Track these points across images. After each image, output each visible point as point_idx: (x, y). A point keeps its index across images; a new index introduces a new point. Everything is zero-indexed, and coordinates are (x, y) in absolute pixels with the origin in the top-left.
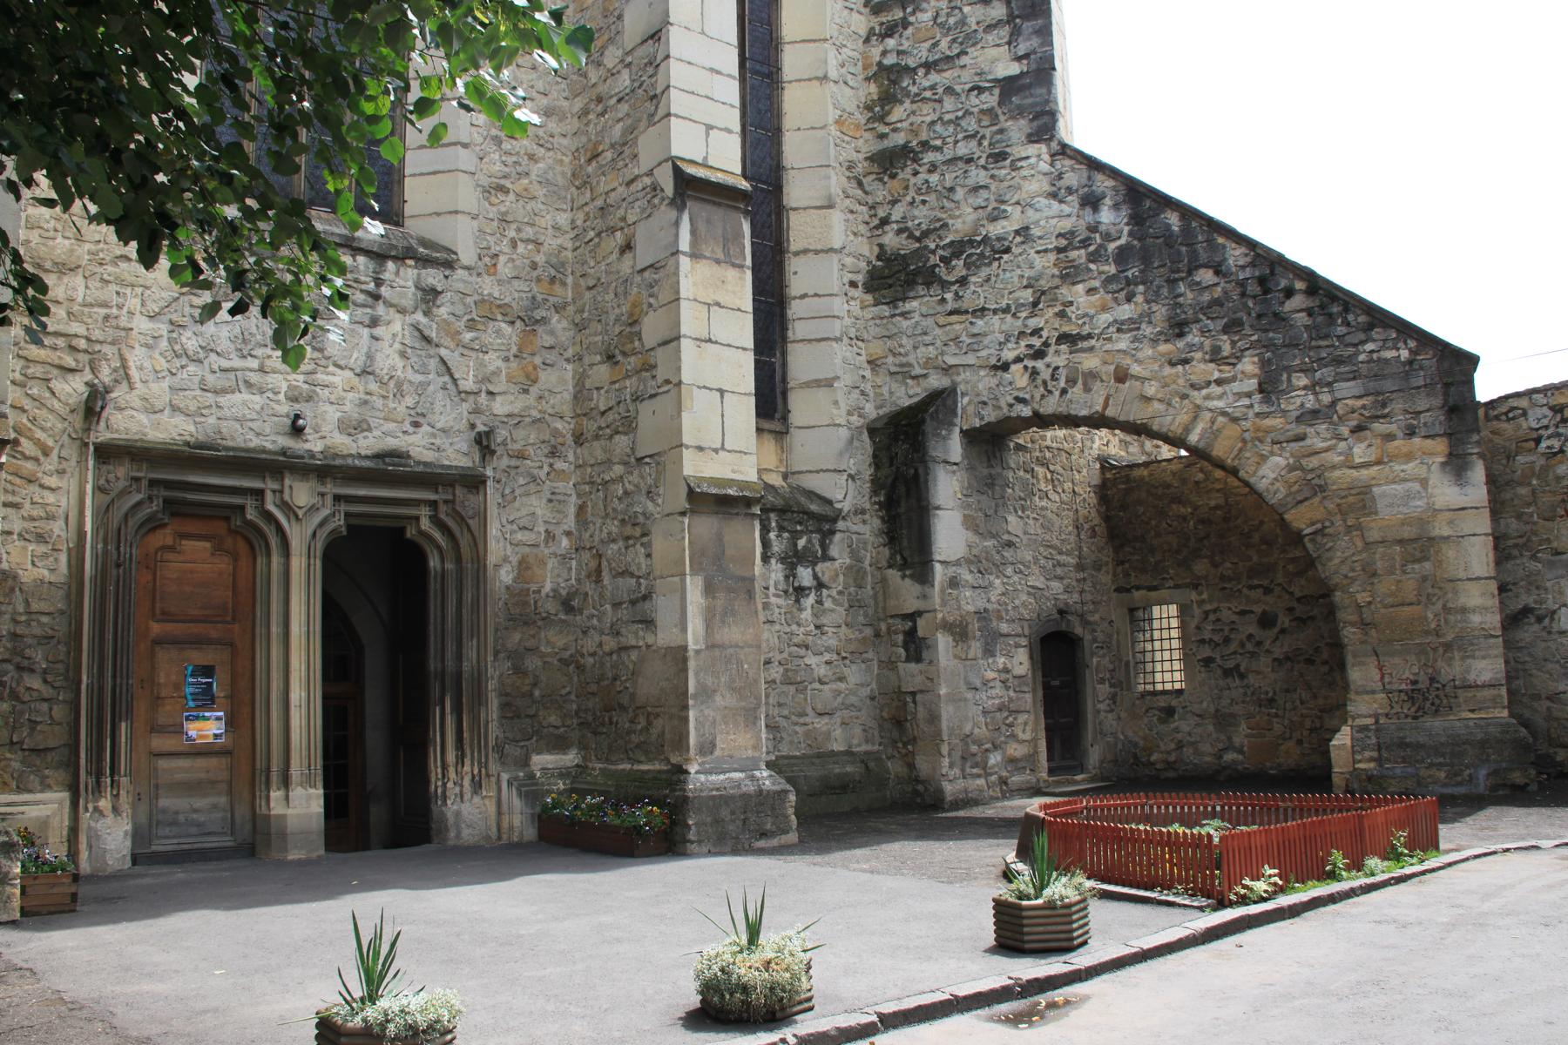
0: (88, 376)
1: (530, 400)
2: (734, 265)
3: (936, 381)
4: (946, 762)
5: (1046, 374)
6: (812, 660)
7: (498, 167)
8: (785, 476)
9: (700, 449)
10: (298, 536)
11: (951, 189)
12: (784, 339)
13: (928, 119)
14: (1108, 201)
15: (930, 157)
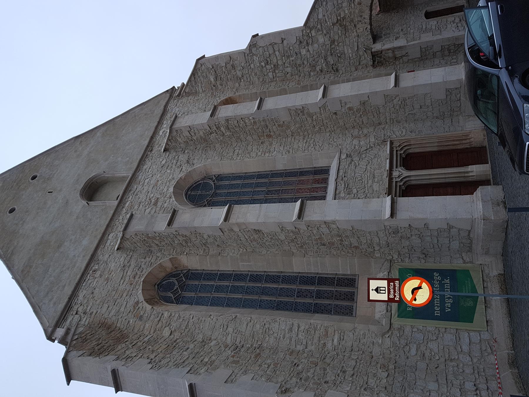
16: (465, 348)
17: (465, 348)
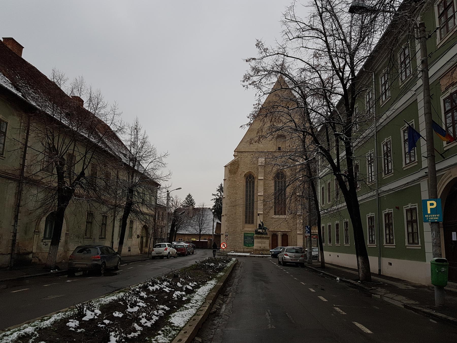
10: (280, 235)
16: (239, 244)
17: (239, 244)
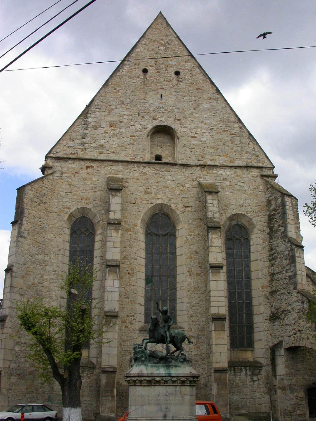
0: (130, 356)
1: (198, 352)
2: (223, 331)
3: (281, 339)
4: (279, 414)
5: (296, 338)
6: (257, 394)
7: (192, 312)
8: (254, 359)
9: (216, 362)
11: (282, 300)
12: (253, 331)
13: (278, 285)
14: (305, 302)
15: (279, 293)
